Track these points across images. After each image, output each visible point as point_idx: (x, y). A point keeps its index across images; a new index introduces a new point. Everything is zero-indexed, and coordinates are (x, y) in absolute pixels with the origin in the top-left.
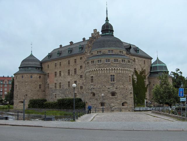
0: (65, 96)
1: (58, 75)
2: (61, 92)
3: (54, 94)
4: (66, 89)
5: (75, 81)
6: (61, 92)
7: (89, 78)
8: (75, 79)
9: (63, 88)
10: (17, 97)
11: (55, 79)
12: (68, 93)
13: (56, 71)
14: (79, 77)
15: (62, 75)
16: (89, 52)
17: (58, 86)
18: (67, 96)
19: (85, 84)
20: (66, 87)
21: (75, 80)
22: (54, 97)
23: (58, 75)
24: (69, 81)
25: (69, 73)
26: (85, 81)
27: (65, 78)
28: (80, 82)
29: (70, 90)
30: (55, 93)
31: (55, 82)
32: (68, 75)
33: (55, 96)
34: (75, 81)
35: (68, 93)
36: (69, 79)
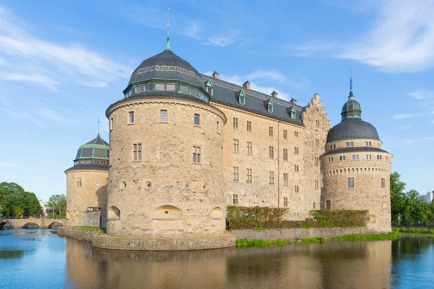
0: (263, 202)
1: (243, 148)
2: (250, 190)
3: (232, 193)
4: (265, 187)
5: (284, 174)
6: (250, 190)
7: (378, 180)
8: (285, 169)
9: (257, 183)
10: (206, 193)
11: (235, 156)
12: (268, 195)
13: (238, 137)
14: (291, 167)
15: (254, 154)
16: (309, 128)
17: (243, 179)
18: (267, 202)
19: (303, 183)
20: (265, 181)
21: (286, 172)
22: (233, 200)
23: (243, 148)
24: (271, 170)
25: (271, 155)
26: (303, 178)
27: (264, 161)
28: (294, 178)
29: (274, 189)
30: (233, 190)
31: (235, 164)
32: (270, 156)
33: (233, 198)
34: (284, 174)
35: (268, 195)
36: (272, 165)
